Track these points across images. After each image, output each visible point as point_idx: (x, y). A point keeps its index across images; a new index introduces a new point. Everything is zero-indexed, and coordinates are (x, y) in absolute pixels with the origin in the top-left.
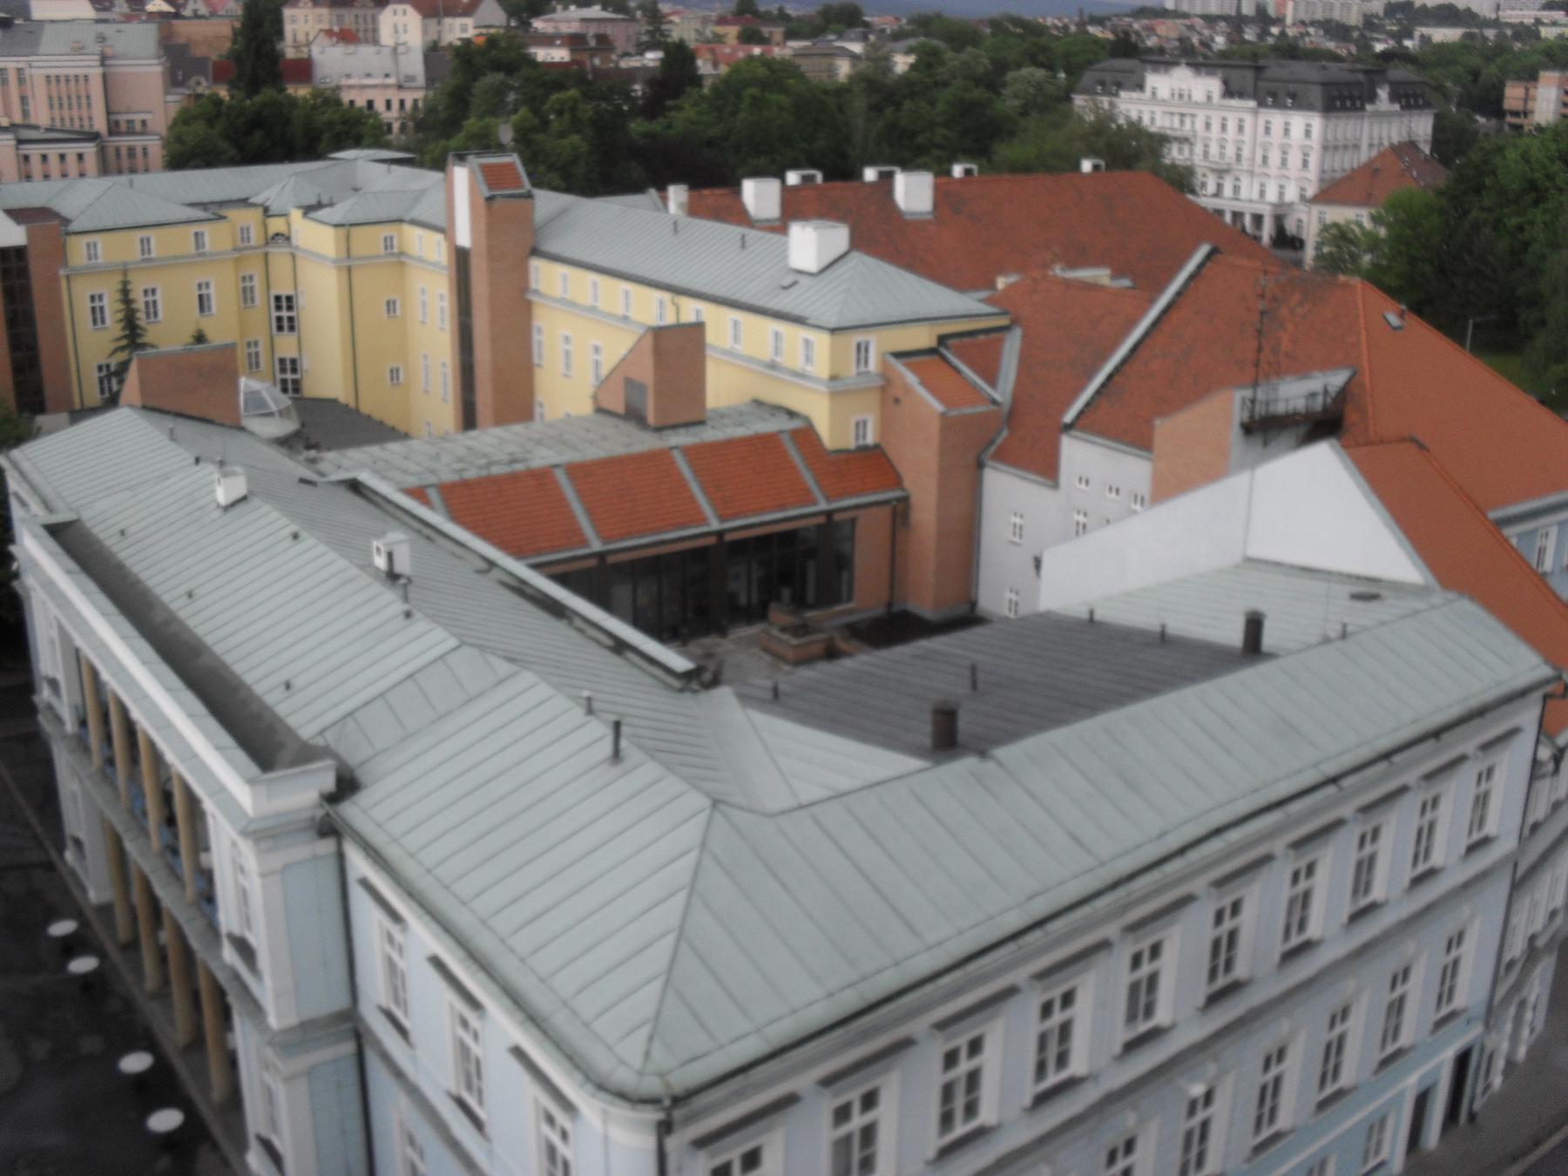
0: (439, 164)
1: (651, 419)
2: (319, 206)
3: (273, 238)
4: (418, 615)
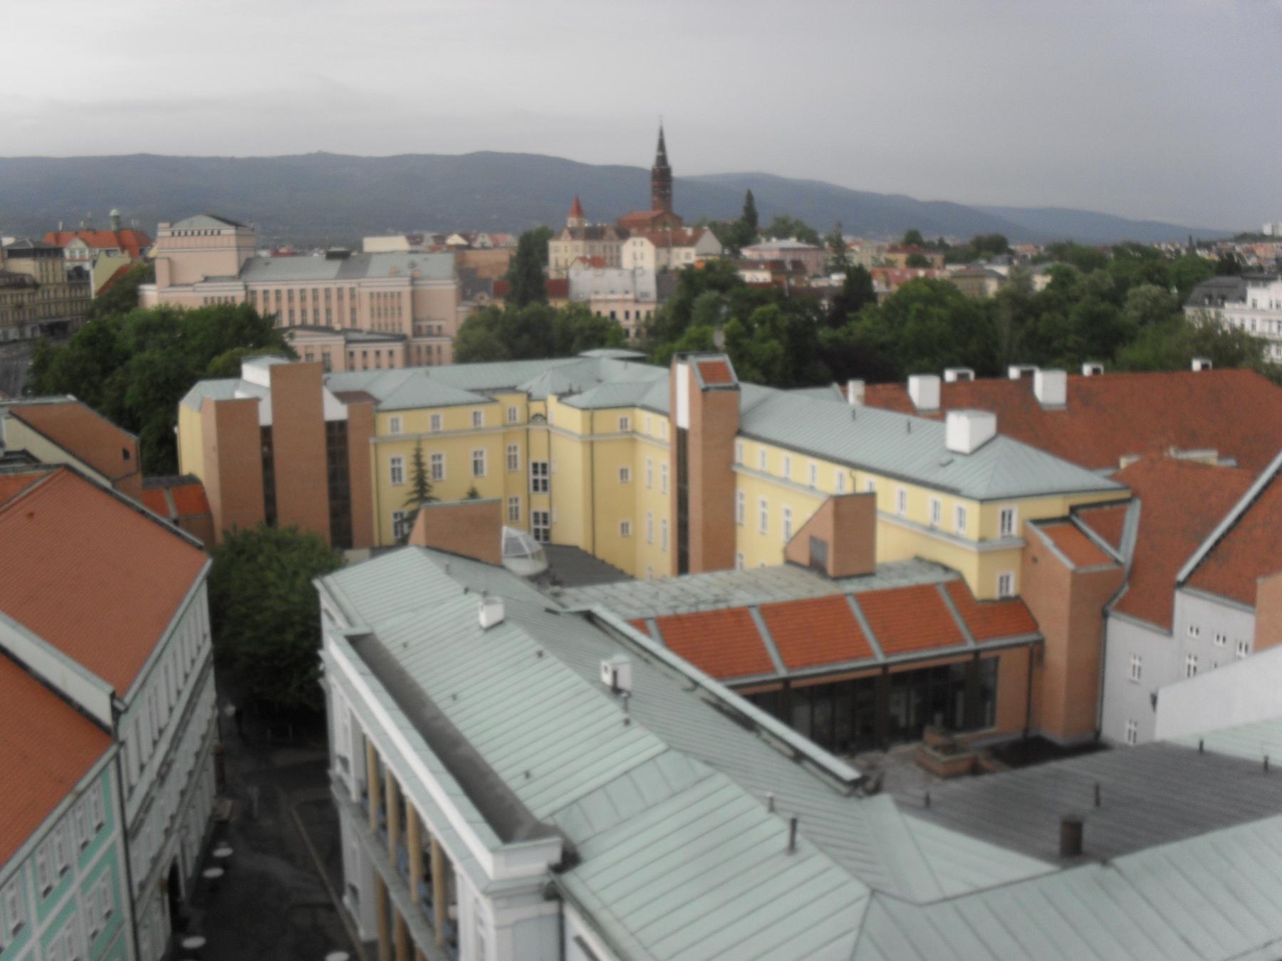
0: (666, 362)
1: (830, 570)
2: (571, 393)
4: (634, 723)
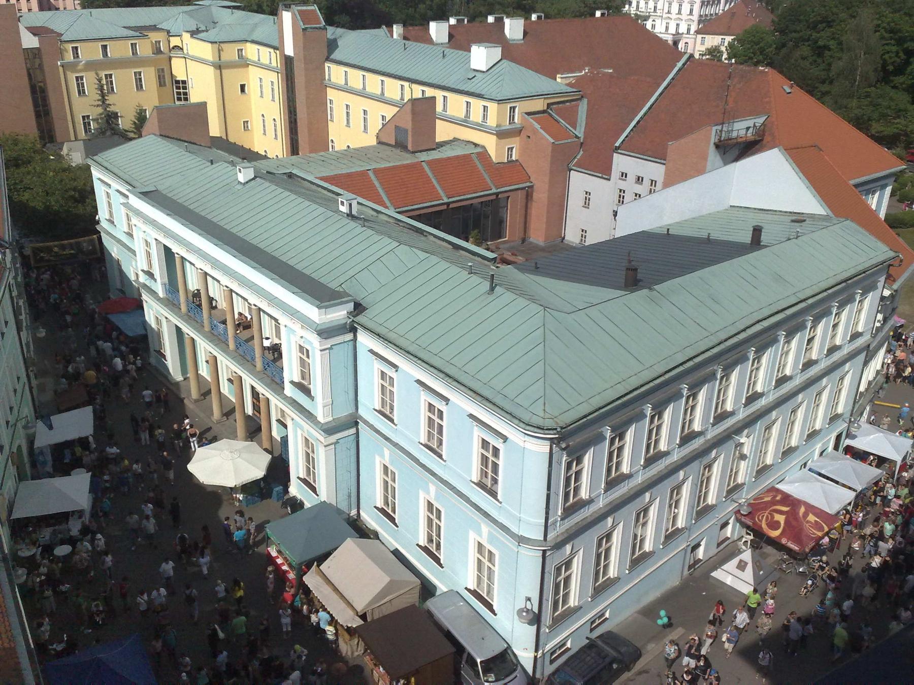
0: (274, 12)
1: (410, 148)
3: (173, 48)
